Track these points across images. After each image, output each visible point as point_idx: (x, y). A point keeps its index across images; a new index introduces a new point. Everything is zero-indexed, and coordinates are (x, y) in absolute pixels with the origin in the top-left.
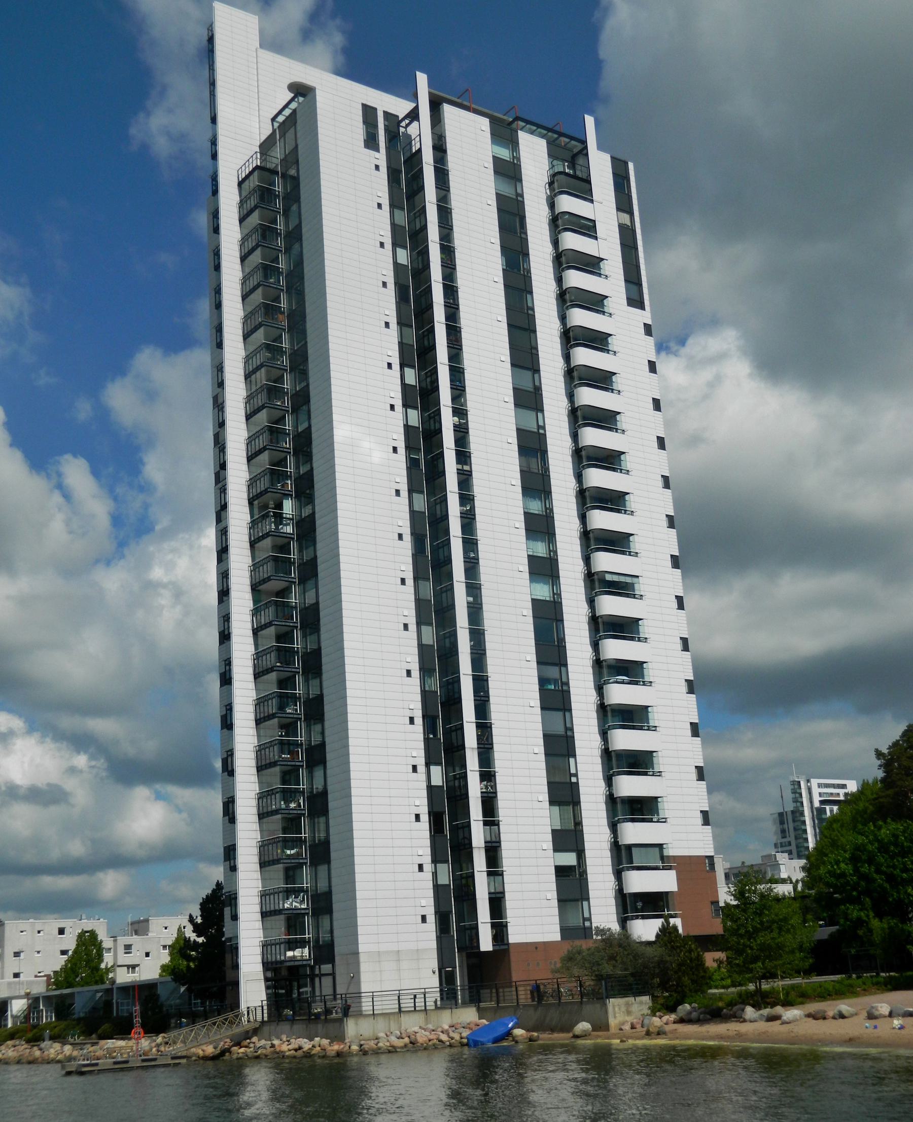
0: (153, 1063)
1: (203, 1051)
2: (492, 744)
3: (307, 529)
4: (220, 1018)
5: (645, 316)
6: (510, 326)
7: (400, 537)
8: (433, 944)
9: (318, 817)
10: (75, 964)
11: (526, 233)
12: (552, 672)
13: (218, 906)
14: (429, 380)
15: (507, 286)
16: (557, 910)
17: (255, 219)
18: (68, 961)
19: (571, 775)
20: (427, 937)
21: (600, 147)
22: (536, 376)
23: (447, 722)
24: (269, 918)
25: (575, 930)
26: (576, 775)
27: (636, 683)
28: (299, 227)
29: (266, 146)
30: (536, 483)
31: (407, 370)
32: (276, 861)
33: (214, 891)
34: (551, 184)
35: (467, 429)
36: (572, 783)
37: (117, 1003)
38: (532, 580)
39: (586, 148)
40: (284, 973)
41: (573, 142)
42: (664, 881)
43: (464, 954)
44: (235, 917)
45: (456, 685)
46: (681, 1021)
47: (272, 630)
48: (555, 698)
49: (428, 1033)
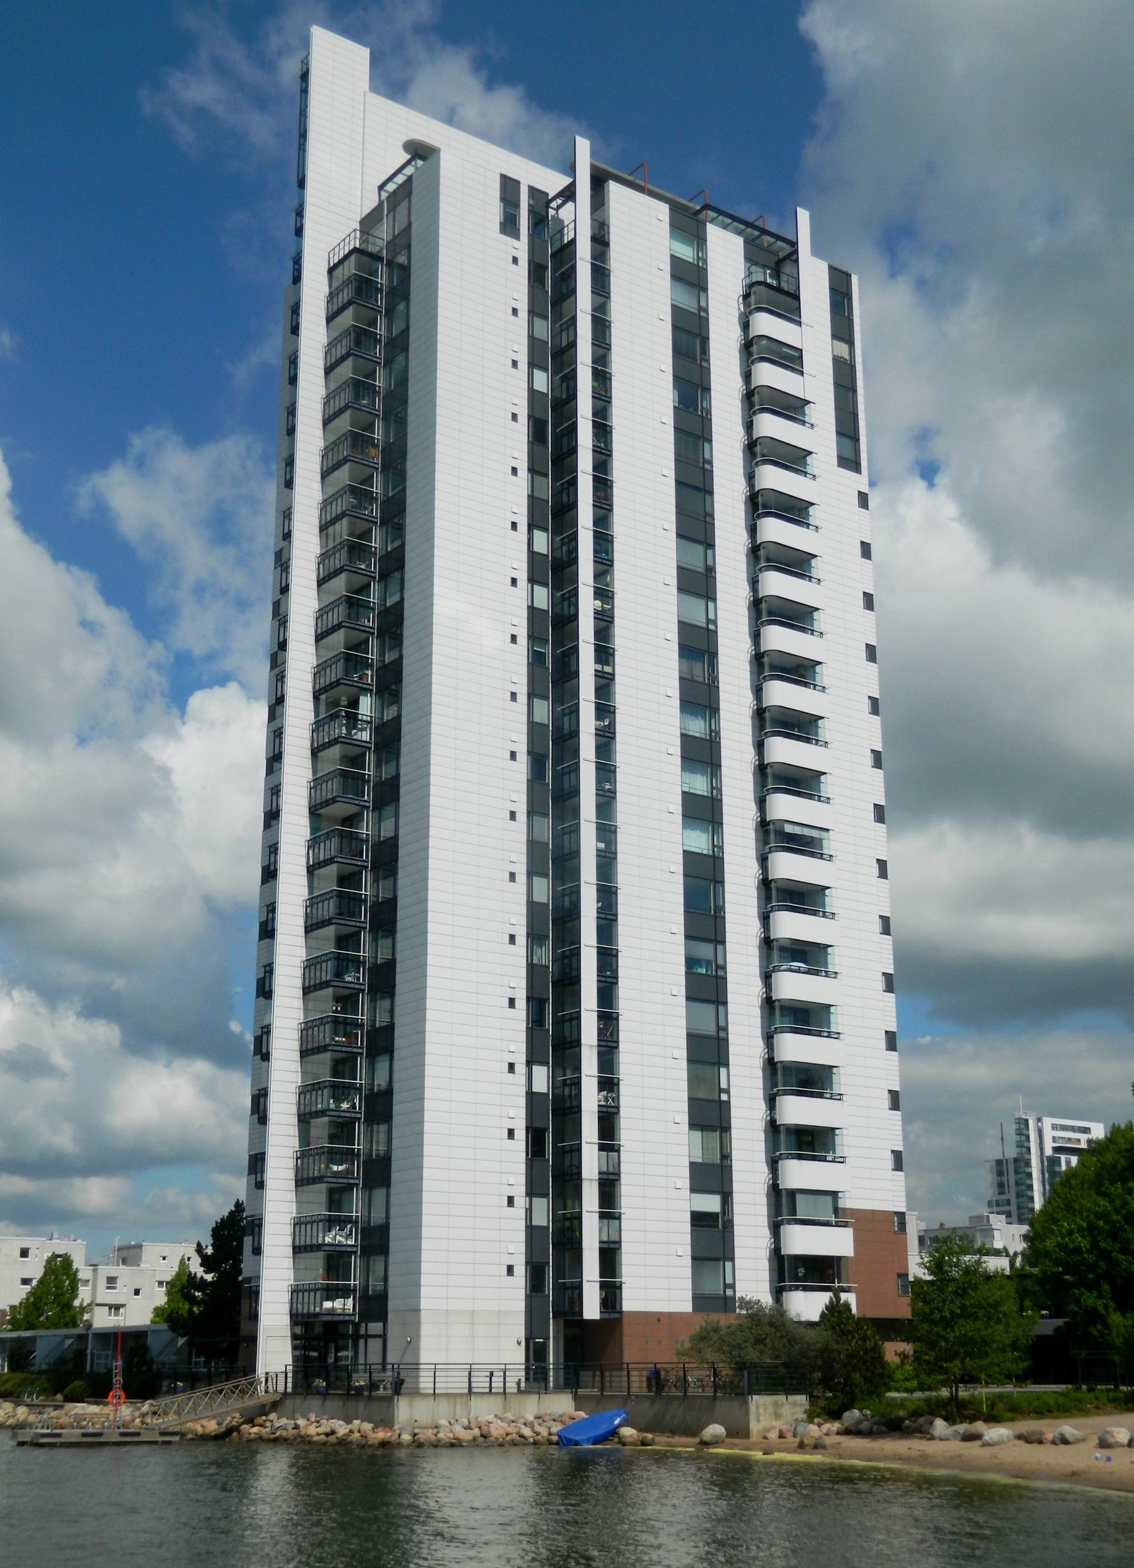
0: (136, 1439)
1: (203, 1427)
2: (617, 1042)
3: (389, 738)
4: (227, 1386)
5: (859, 482)
6: (679, 483)
7: (513, 756)
8: (521, 1306)
9: (378, 1124)
10: (40, 1299)
11: (708, 361)
12: (705, 950)
13: (235, 1235)
14: (565, 548)
15: (677, 429)
16: (690, 1270)
17: (347, 319)
18: (30, 1294)
19: (721, 1091)
20: (514, 1294)
21: (816, 252)
22: (709, 552)
23: (558, 1008)
24: (304, 1255)
25: (713, 1300)
26: (727, 1091)
27: (816, 973)
28: (406, 331)
29: (369, 223)
30: (699, 697)
32: (318, 1180)
33: (231, 1213)
34: (746, 297)
35: (613, 618)
36: (720, 1101)
37: (92, 1355)
39: (796, 252)
40: (318, 1330)
41: (779, 243)
42: (836, 1242)
43: (561, 1322)
44: (257, 1251)
45: (574, 959)
46: (847, 1432)
47: (332, 870)
48: (706, 986)
49: (505, 1425)
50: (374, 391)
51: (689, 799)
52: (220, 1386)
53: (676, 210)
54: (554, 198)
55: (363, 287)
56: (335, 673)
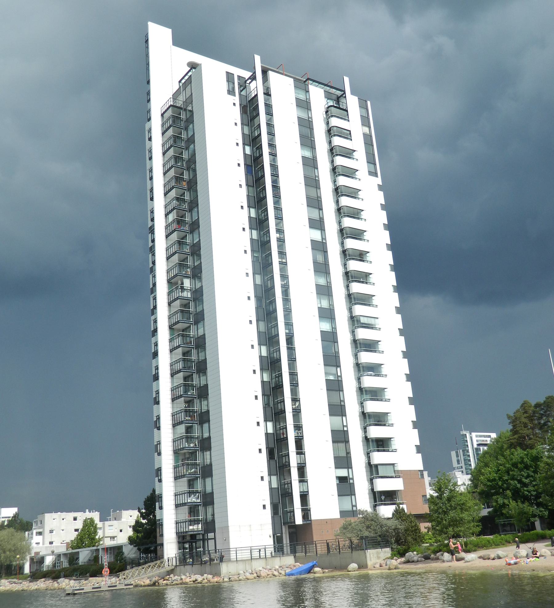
3: (198, 295)
4: (152, 564)
13: (152, 503)
14: (263, 215)
17: (170, 132)
19: (344, 426)
21: (353, 93)
26: (347, 426)
29: (175, 96)
30: (322, 268)
31: (251, 209)
32: (183, 476)
33: (151, 494)
34: (327, 112)
36: (344, 431)
37: (102, 557)
38: (320, 320)
39: (345, 93)
40: (188, 538)
42: (396, 484)
44: (161, 508)
45: (280, 378)
47: (180, 350)
49: (267, 571)
50: (183, 160)
51: (320, 309)
52: (149, 564)
53: (295, 80)
54: (248, 79)
55: (176, 119)
56: (175, 271)
